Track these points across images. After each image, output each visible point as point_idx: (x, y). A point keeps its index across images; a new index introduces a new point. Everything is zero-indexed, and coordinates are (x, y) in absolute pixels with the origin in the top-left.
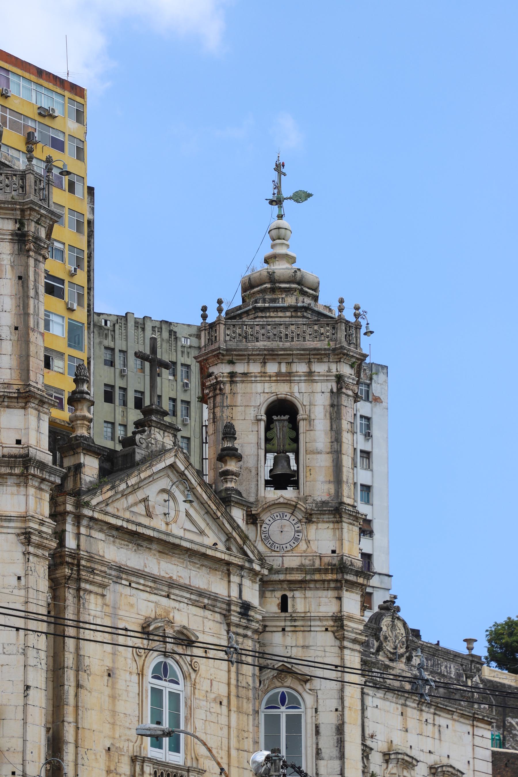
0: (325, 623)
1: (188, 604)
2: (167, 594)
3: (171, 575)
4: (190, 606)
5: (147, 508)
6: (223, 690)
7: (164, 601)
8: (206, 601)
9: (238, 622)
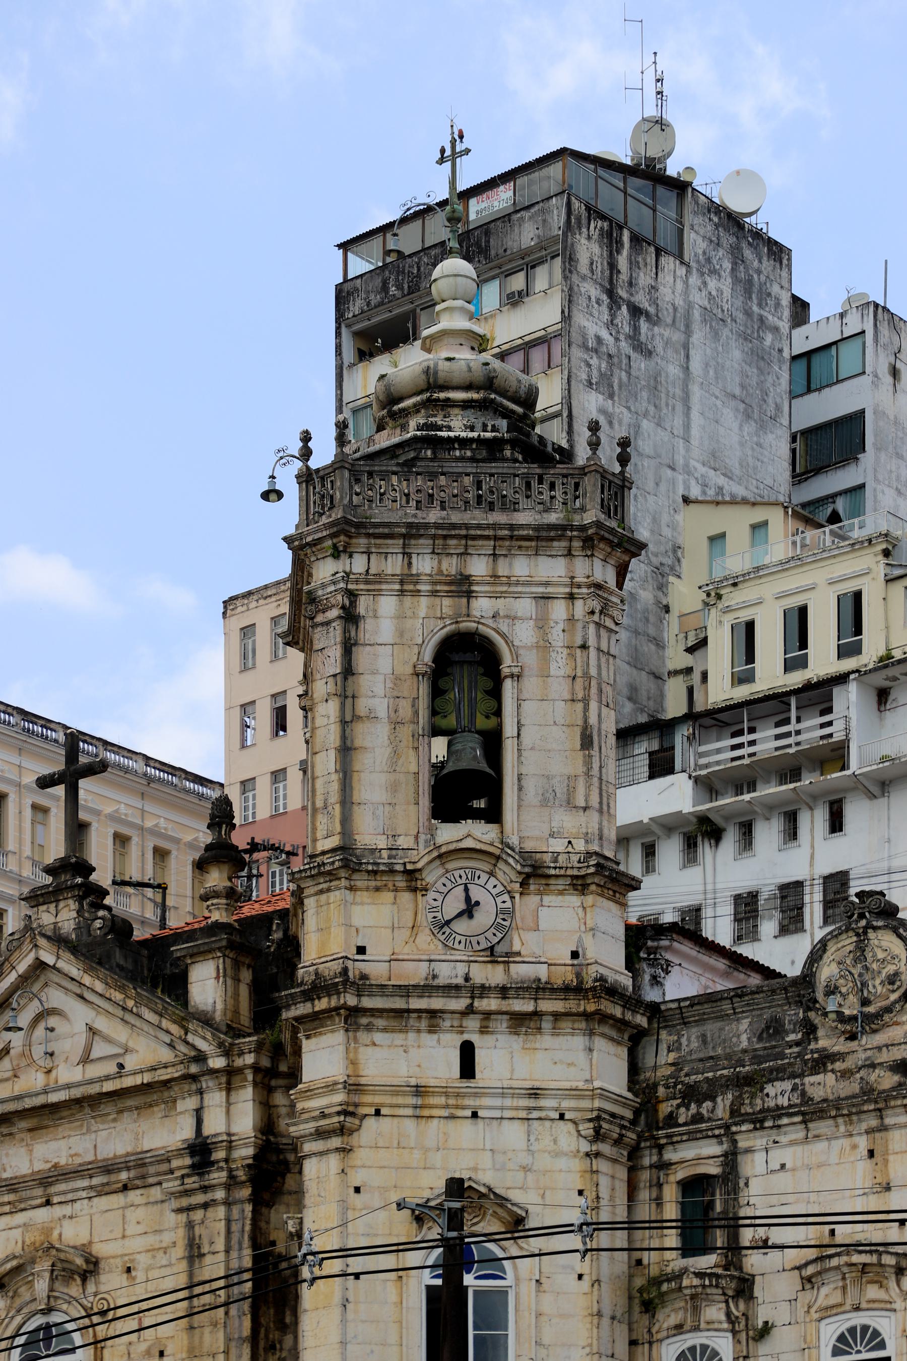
1: (90, 1198)
2: (44, 1200)
3: (56, 1160)
4: (95, 1200)
7: (42, 1215)
8: (124, 1176)
9: (181, 1188)
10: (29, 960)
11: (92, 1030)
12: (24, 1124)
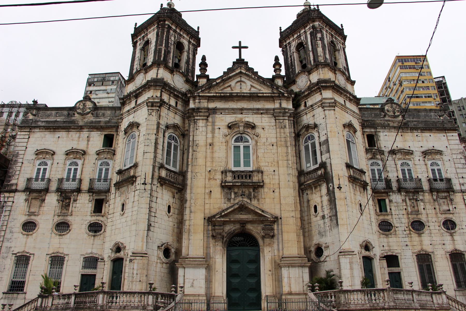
0: (318, 105)
5: (231, 88)
6: (274, 140)
7: (240, 116)
8: (262, 111)
10: (239, 71)
11: (252, 86)
12: (236, 99)
